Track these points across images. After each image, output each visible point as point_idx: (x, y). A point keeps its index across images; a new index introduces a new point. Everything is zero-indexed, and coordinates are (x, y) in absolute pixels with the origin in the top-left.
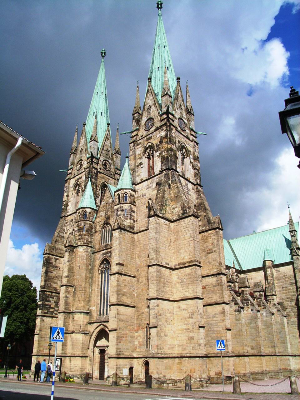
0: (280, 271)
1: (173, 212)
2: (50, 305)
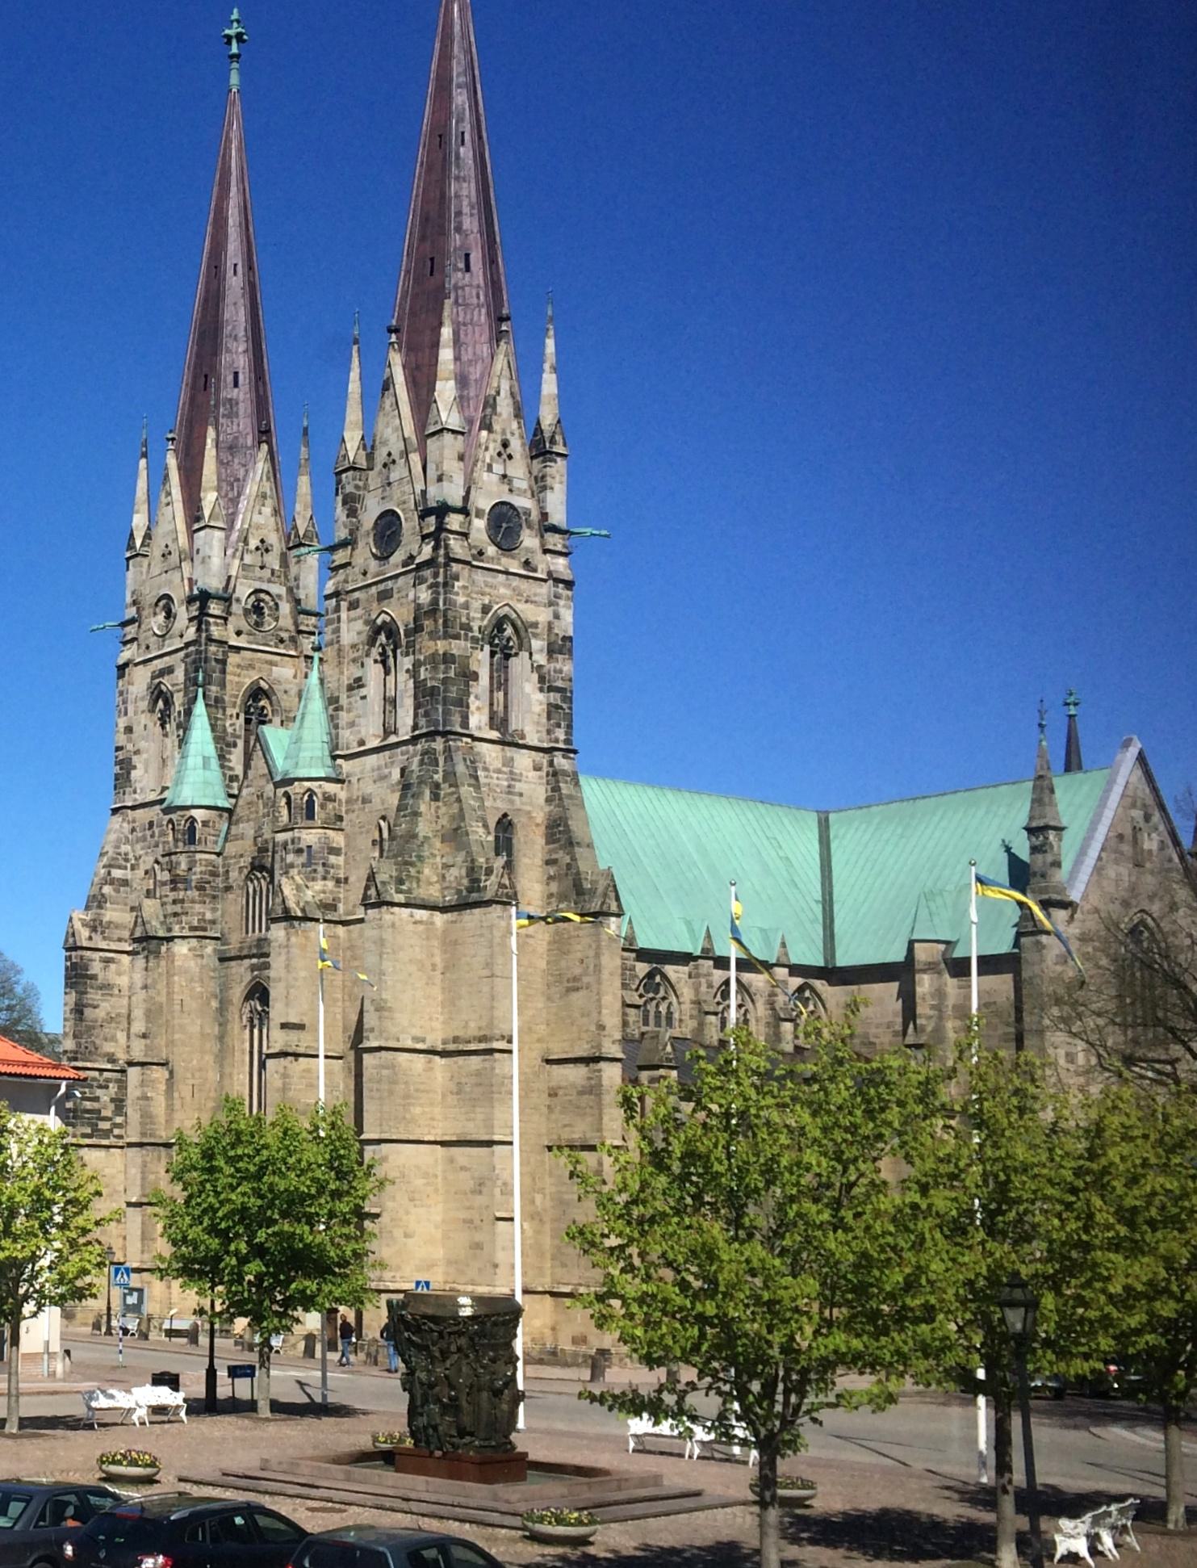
1: (444, 877)
2: (99, 1111)
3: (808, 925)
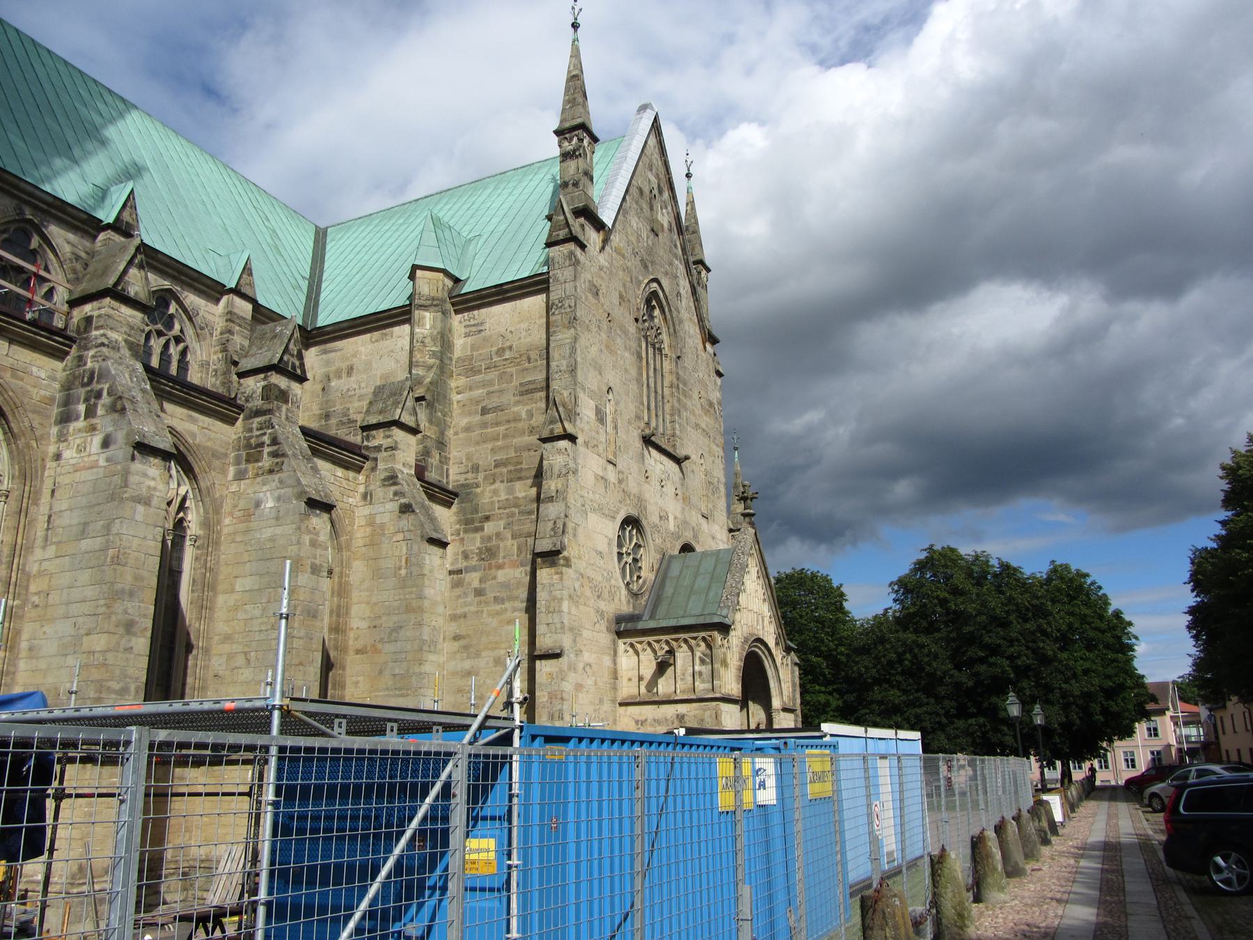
0: (487, 326)
3: (290, 289)
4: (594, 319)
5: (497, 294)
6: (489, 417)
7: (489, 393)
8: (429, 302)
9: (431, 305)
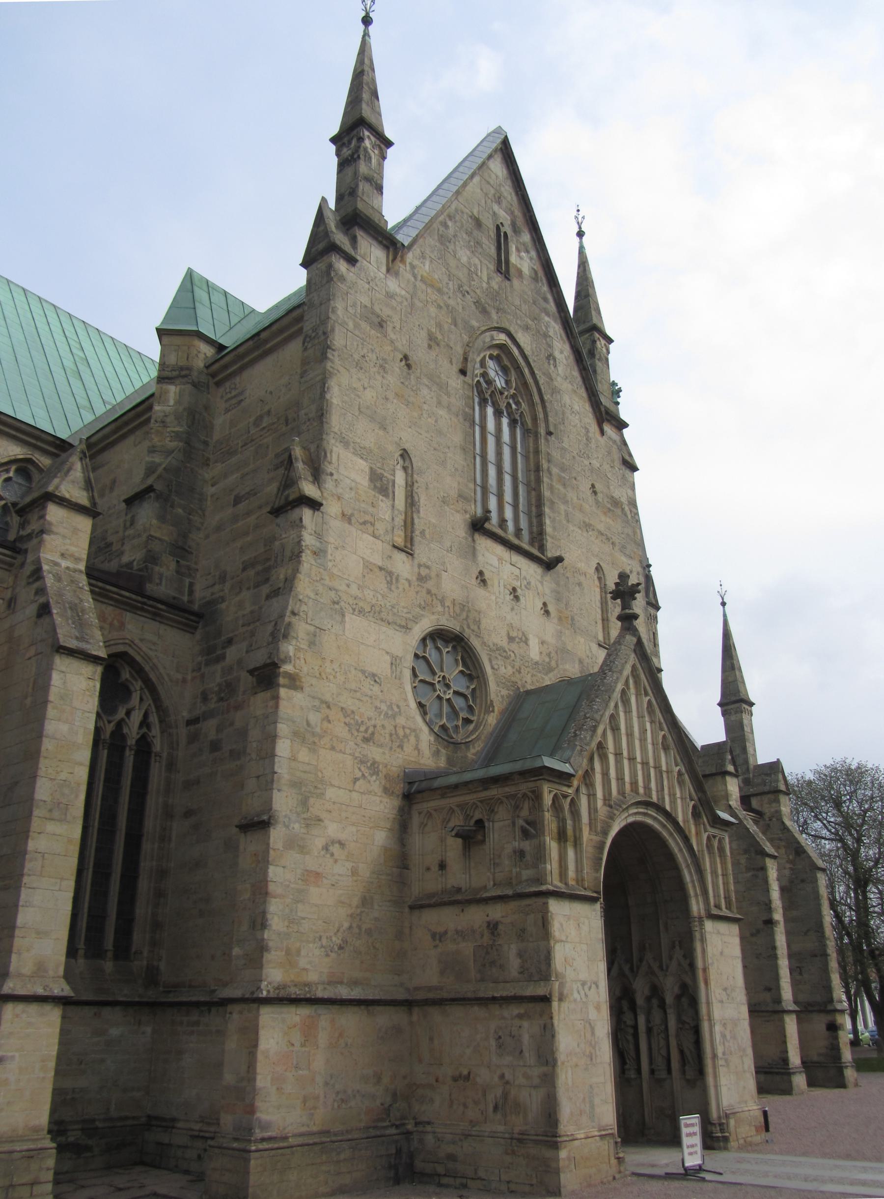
4: (372, 356)
5: (256, 347)
6: (241, 506)
7: (243, 477)
8: (175, 373)
9: (180, 376)
